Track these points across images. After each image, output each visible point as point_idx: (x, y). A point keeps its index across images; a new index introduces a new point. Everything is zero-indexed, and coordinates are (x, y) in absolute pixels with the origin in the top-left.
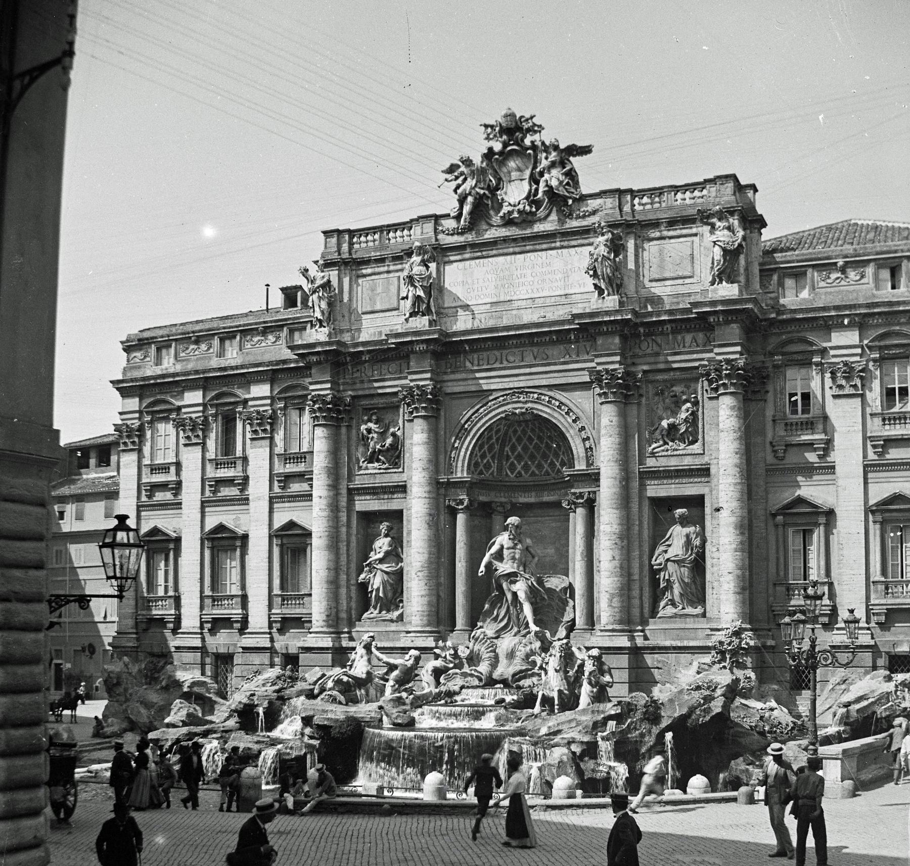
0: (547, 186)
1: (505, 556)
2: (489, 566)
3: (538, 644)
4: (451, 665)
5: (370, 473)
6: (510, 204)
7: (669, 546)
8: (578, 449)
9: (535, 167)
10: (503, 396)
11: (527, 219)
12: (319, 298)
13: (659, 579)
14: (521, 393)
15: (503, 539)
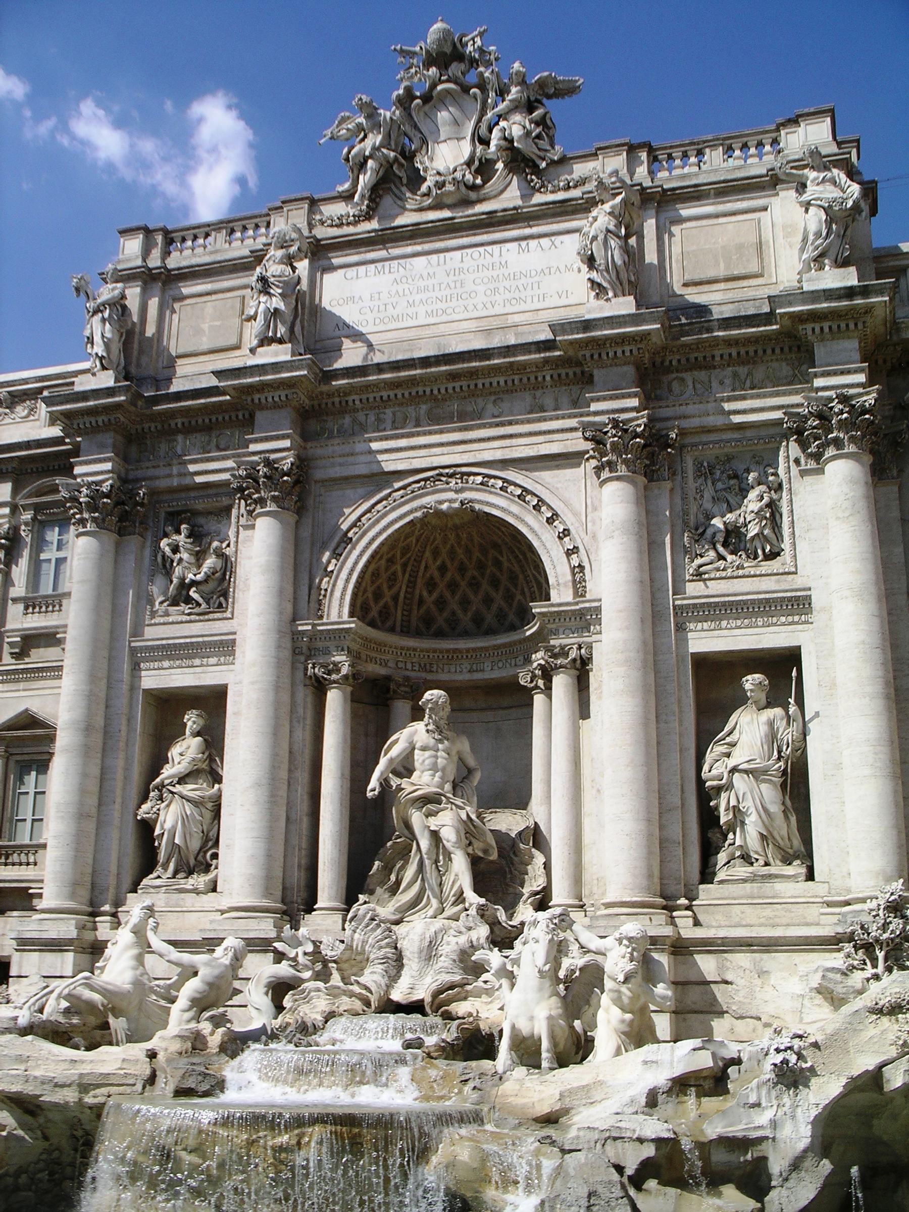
0: (505, 139)
1: (417, 764)
2: (385, 784)
3: (483, 931)
4: (307, 974)
5: (171, 626)
6: (439, 173)
7: (733, 745)
8: (557, 569)
9: (483, 113)
10: (418, 482)
11: (468, 194)
12: (104, 320)
13: (717, 808)
14: (451, 476)
15: (416, 733)
